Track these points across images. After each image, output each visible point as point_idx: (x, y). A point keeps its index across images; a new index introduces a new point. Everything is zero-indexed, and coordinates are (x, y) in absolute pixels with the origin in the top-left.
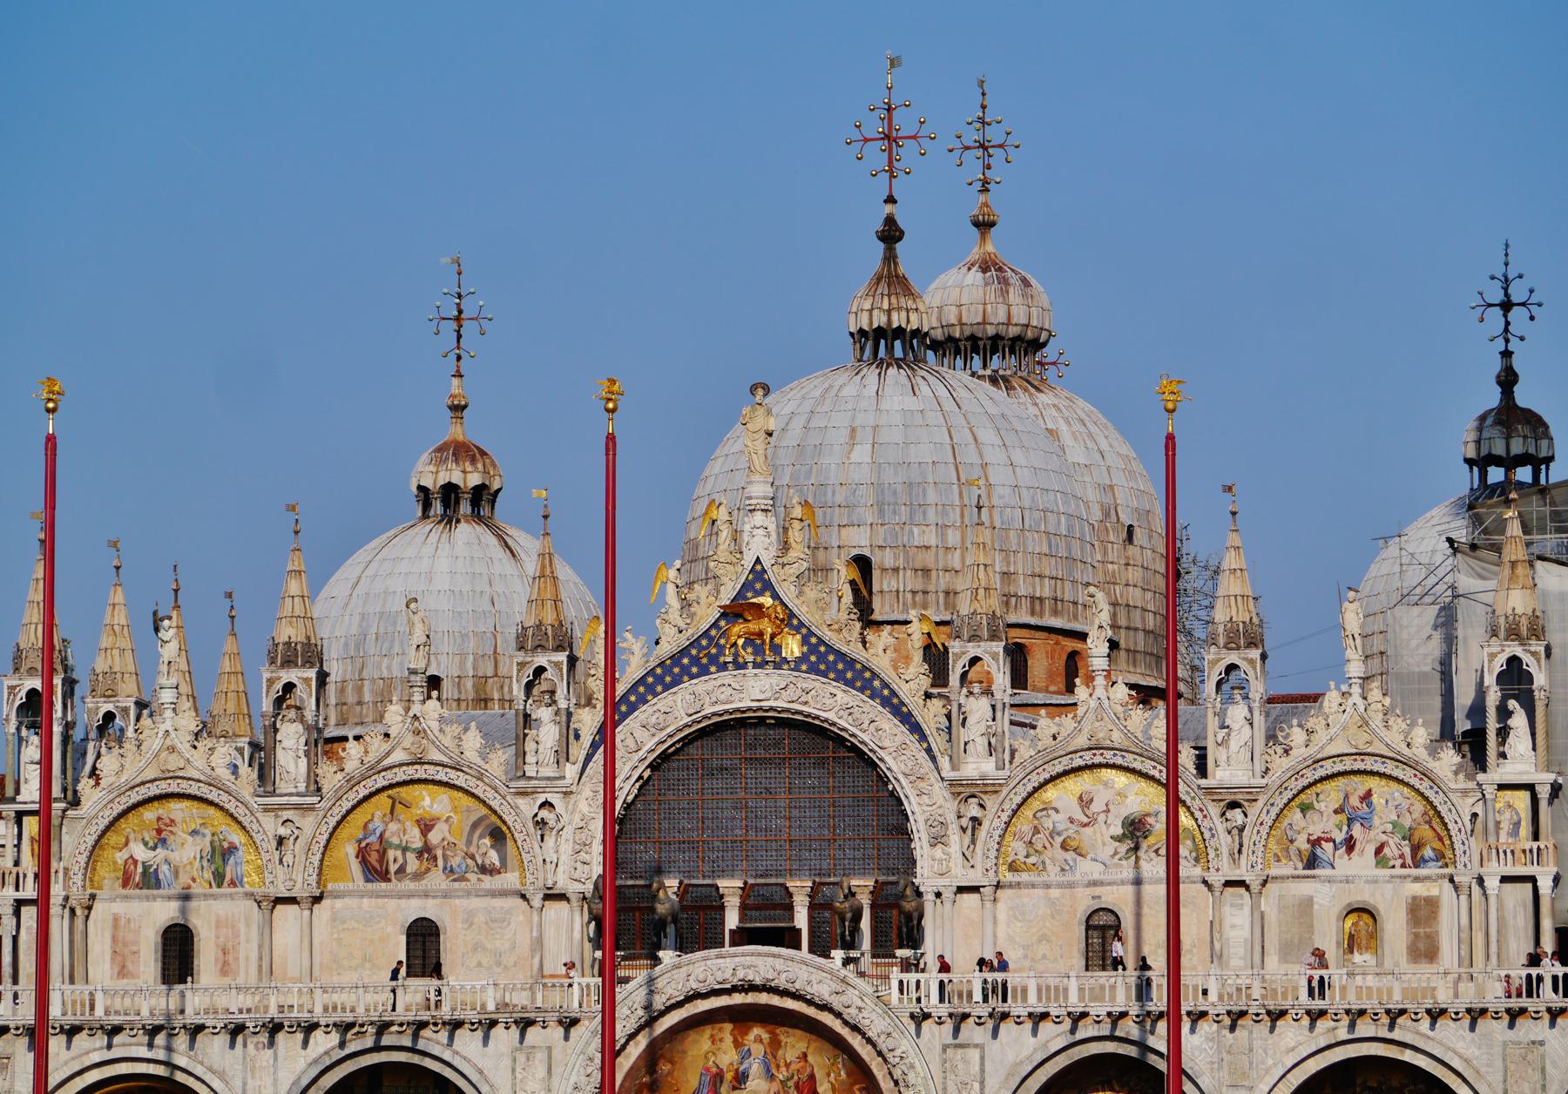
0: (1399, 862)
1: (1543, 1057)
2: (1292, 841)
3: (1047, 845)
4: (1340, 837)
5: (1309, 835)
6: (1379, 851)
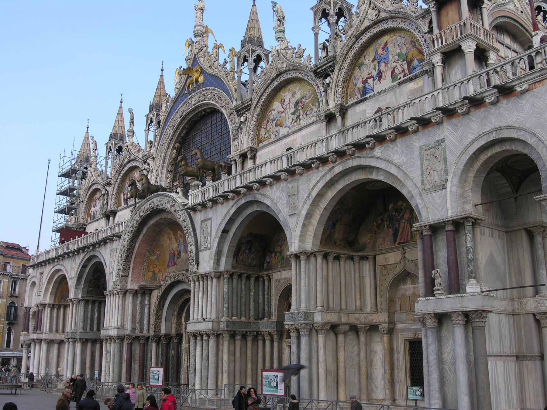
0: (403, 74)
1: (444, 150)
2: (355, 86)
3: (271, 127)
4: (375, 73)
5: (363, 78)
6: (393, 72)
